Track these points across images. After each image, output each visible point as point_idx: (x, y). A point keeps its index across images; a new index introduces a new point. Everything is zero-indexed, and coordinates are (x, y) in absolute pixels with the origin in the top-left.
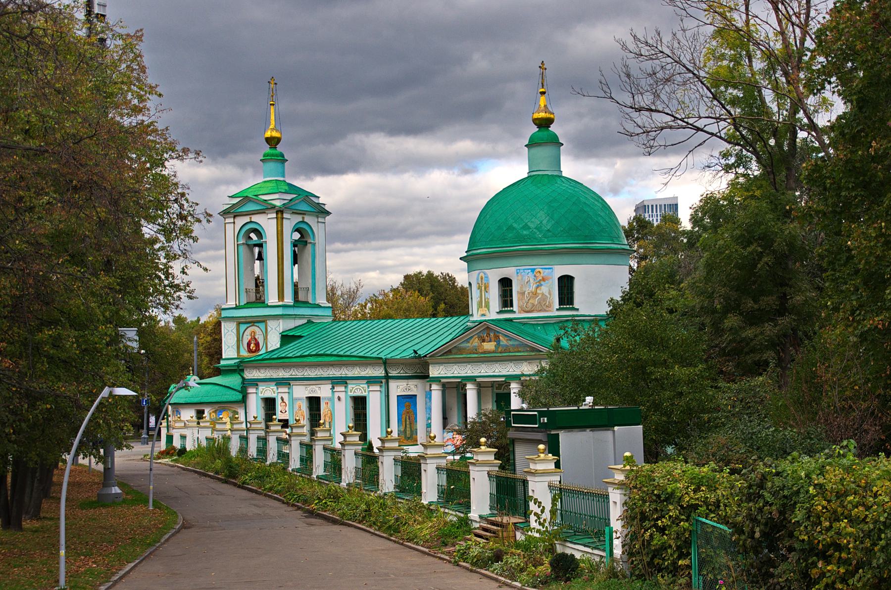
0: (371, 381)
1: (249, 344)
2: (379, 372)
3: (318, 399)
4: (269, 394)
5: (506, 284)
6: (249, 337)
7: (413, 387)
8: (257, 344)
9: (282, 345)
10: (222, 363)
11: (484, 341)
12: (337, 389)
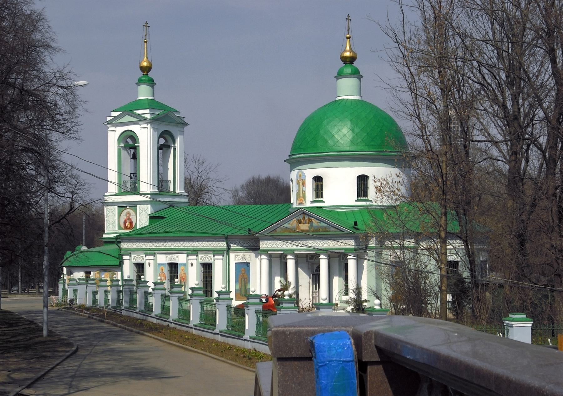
0: (216, 252)
1: (125, 223)
2: (222, 245)
4: (139, 261)
5: (318, 180)
6: (125, 217)
7: (249, 256)
8: (131, 223)
9: (150, 223)
11: (300, 223)
12: (190, 257)
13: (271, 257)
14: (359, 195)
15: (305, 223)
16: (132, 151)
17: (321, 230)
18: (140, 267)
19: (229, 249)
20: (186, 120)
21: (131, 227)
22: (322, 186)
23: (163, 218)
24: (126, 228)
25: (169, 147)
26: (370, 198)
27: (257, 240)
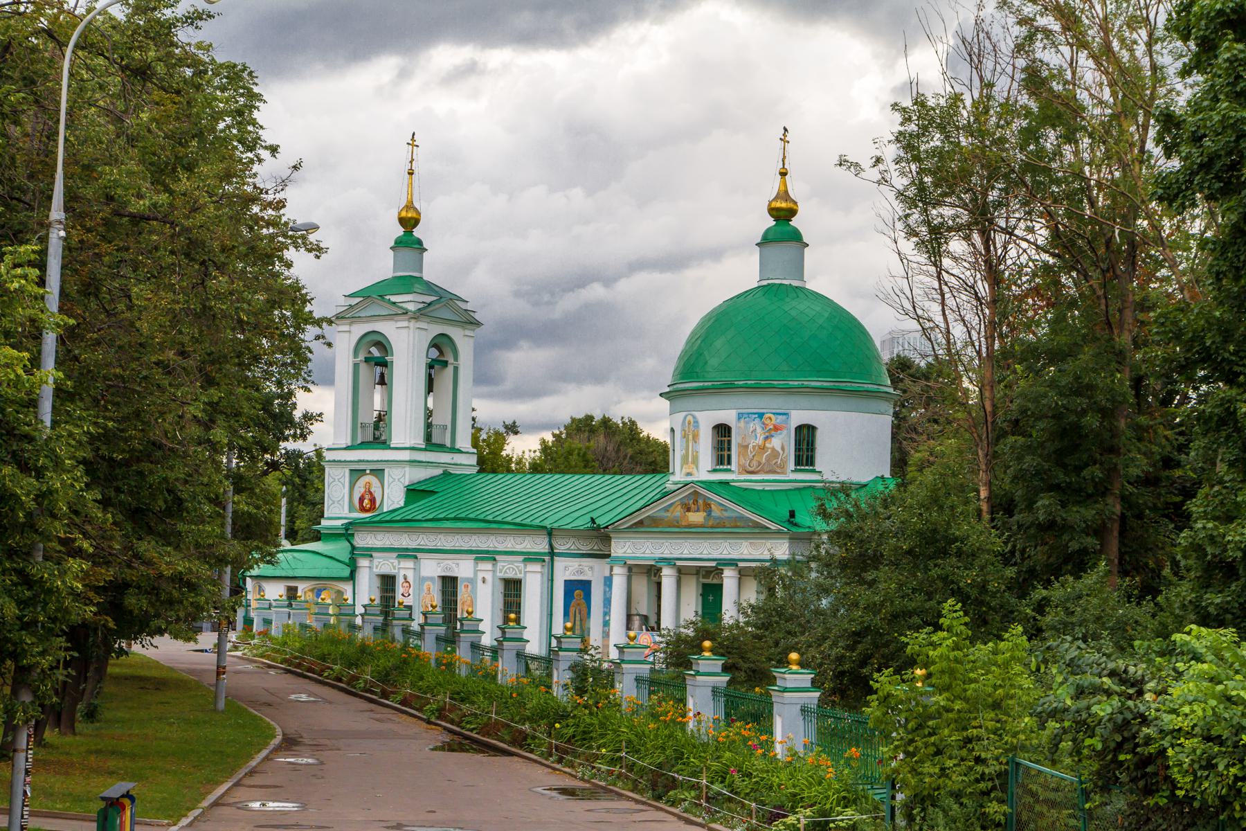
0: (530, 558)
1: (361, 500)
3: (454, 580)
4: (387, 569)
5: (722, 431)
6: (363, 490)
7: (592, 571)
8: (373, 501)
10: (324, 523)
11: (689, 510)
13: (632, 570)
14: (798, 462)
15: (698, 510)
16: (379, 369)
17: (727, 524)
18: (388, 582)
19: (552, 554)
20: (477, 316)
21: (373, 507)
22: (729, 442)
23: (433, 492)
24: (363, 509)
25: (445, 364)
26: (817, 468)
27: (606, 539)
